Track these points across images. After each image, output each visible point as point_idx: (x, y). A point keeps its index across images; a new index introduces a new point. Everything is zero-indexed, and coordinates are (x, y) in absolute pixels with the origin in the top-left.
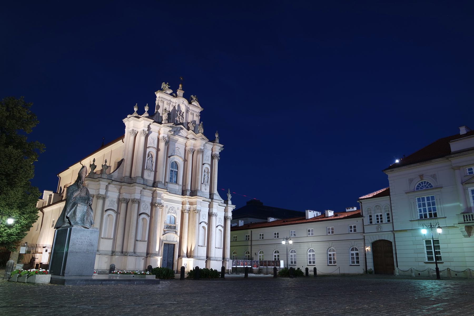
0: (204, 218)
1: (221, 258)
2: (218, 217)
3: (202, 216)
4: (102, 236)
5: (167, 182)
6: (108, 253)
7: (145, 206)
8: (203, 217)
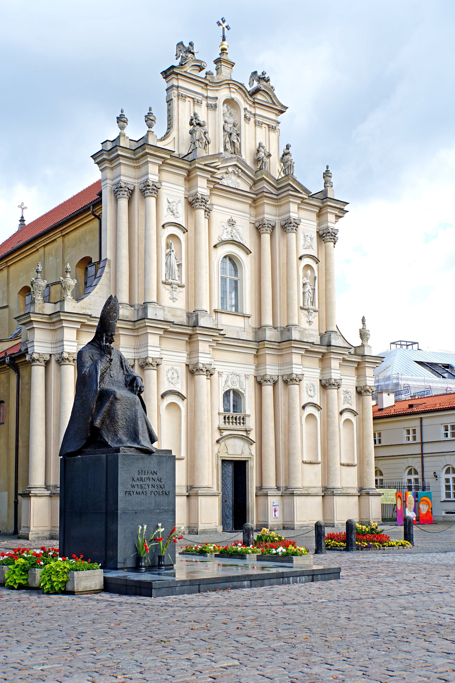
0: (312, 393)
2: (341, 389)
8: (309, 392)
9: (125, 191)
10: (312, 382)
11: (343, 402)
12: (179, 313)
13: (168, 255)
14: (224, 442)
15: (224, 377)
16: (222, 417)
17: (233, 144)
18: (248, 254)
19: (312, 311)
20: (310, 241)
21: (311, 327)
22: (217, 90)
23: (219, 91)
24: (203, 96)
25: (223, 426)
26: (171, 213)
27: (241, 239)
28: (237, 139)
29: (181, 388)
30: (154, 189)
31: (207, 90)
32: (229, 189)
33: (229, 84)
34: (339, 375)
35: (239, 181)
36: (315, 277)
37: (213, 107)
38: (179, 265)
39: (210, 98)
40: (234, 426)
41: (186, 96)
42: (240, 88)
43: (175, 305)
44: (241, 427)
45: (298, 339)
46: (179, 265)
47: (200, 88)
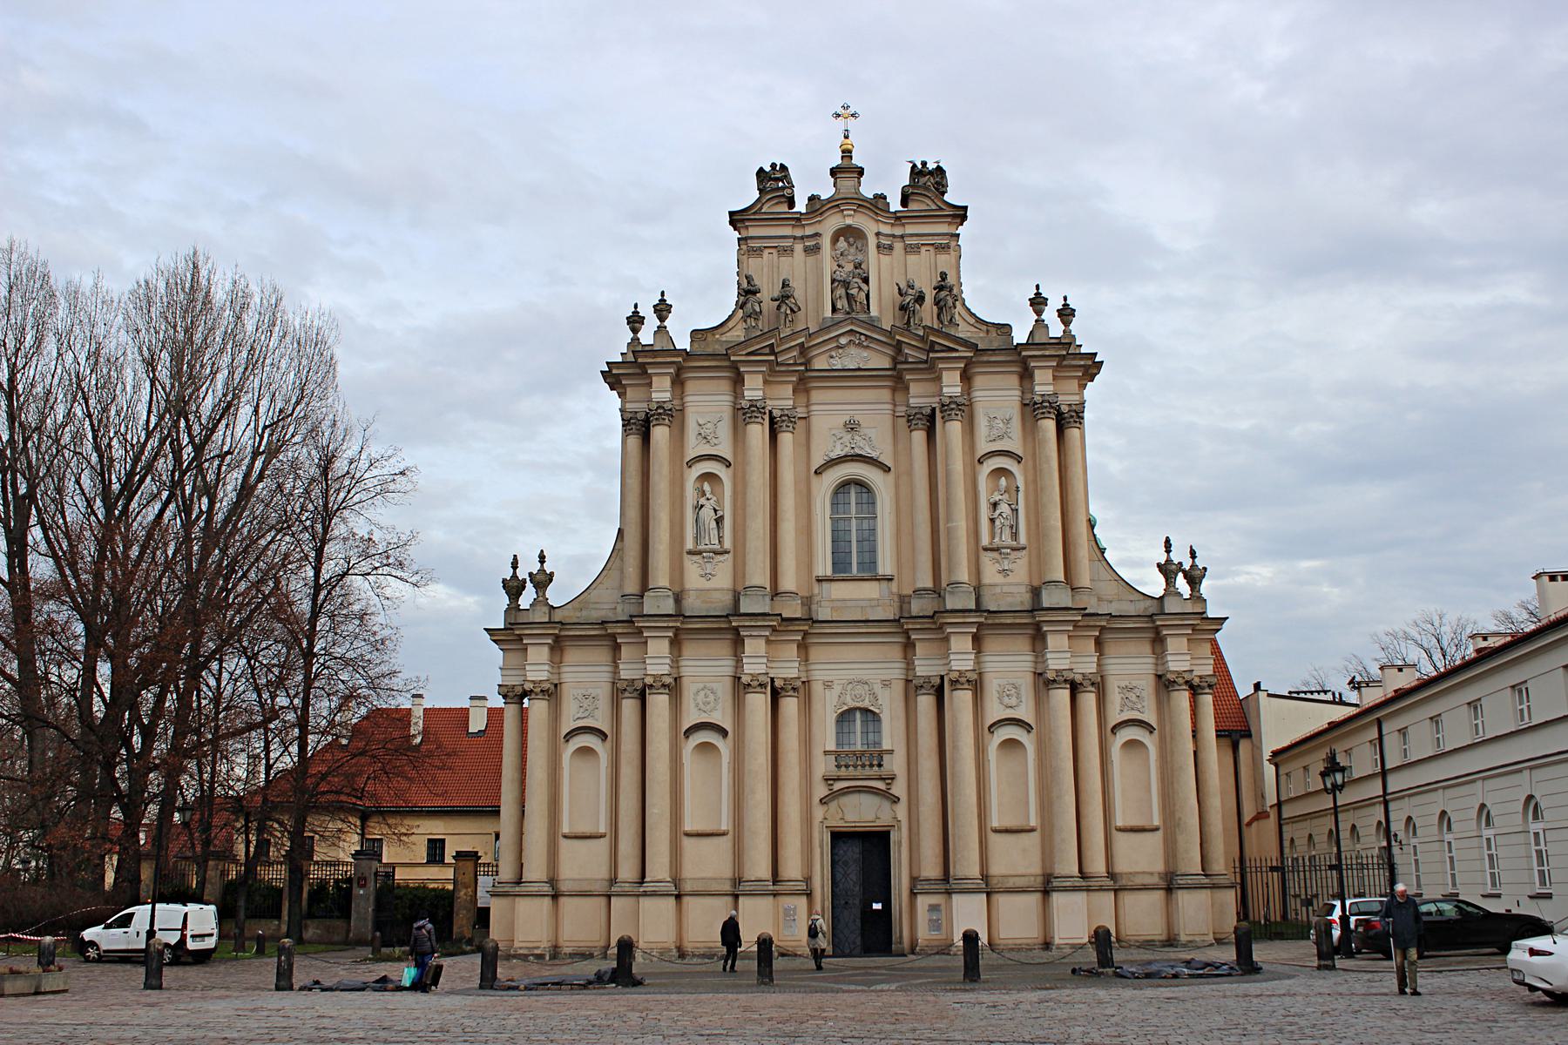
0: (1013, 701)
1: (1152, 874)
3: (995, 695)
4: (566, 829)
5: (819, 580)
6: (592, 889)
7: (706, 696)
9: (634, 424)
10: (1011, 681)
12: (717, 595)
14: (836, 802)
15: (837, 689)
17: (849, 297)
18: (885, 471)
20: (1001, 425)
21: (1010, 579)
23: (823, 223)
24: (795, 238)
25: (834, 772)
26: (705, 441)
27: (873, 448)
28: (860, 289)
29: (722, 717)
30: (660, 414)
31: (803, 226)
32: (836, 374)
36: (1018, 487)
37: (813, 250)
39: (808, 237)
40: (859, 772)
41: (761, 249)
43: (708, 585)
47: (790, 228)
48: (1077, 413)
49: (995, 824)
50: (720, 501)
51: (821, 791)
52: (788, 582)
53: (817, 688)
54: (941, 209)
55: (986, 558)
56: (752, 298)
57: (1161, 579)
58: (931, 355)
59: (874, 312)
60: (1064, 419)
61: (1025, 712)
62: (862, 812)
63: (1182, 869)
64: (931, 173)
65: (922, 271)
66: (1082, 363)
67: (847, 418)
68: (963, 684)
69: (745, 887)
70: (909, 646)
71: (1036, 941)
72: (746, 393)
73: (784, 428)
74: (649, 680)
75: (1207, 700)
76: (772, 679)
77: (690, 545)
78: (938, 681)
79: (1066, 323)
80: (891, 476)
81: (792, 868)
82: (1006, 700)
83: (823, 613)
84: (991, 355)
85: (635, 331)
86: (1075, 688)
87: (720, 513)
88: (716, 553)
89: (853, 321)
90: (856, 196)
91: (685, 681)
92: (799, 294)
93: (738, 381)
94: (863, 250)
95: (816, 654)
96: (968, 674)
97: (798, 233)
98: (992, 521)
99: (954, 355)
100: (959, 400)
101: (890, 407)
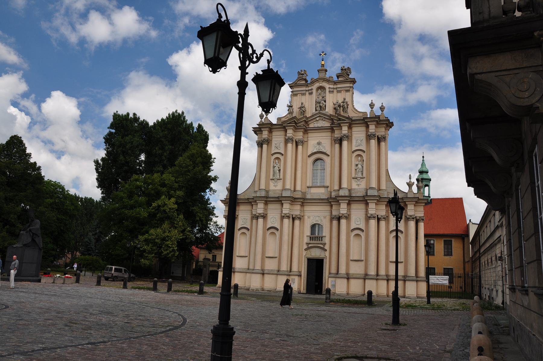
0: (359, 223)
3: (354, 221)
5: (308, 187)
10: (358, 217)
11: (393, 226)
13: (274, 167)
16: (309, 238)
17: (320, 106)
19: (359, 179)
20: (359, 142)
22: (313, 85)
24: (306, 90)
25: (309, 242)
27: (325, 149)
31: (309, 87)
33: (318, 80)
34: (375, 211)
35: (324, 122)
37: (311, 94)
38: (279, 170)
40: (316, 242)
42: (324, 80)
44: (320, 242)
45: (343, 195)
46: (279, 170)
48: (384, 138)
49: (351, 258)
50: (280, 165)
51: (305, 247)
52: (298, 188)
53: (306, 217)
54: (347, 79)
55: (353, 181)
56: (291, 108)
57: (407, 187)
58: (339, 122)
59: (327, 110)
60: (380, 139)
61: (362, 226)
62: (316, 254)
63: (409, 275)
64: (345, 70)
65: (339, 98)
66: (385, 122)
67: (318, 141)
68: (343, 217)
69: (280, 273)
70: (331, 206)
71: (361, 293)
72: (287, 135)
73: (299, 144)
74: (257, 215)
75: (421, 225)
76: (292, 215)
77: (271, 177)
78: (338, 216)
79: (382, 111)
80: (330, 157)
81: (295, 268)
82: (357, 223)
83: (308, 197)
84: (357, 121)
85: (262, 118)
86: (379, 220)
87: (280, 168)
88: (278, 179)
89: (320, 113)
90: (324, 77)
91: (268, 215)
92: (306, 106)
93: (286, 131)
94: (325, 93)
95: (307, 208)
96: (345, 215)
97: (307, 89)
98: (356, 170)
99: (345, 121)
100: (347, 135)
101: (330, 137)
